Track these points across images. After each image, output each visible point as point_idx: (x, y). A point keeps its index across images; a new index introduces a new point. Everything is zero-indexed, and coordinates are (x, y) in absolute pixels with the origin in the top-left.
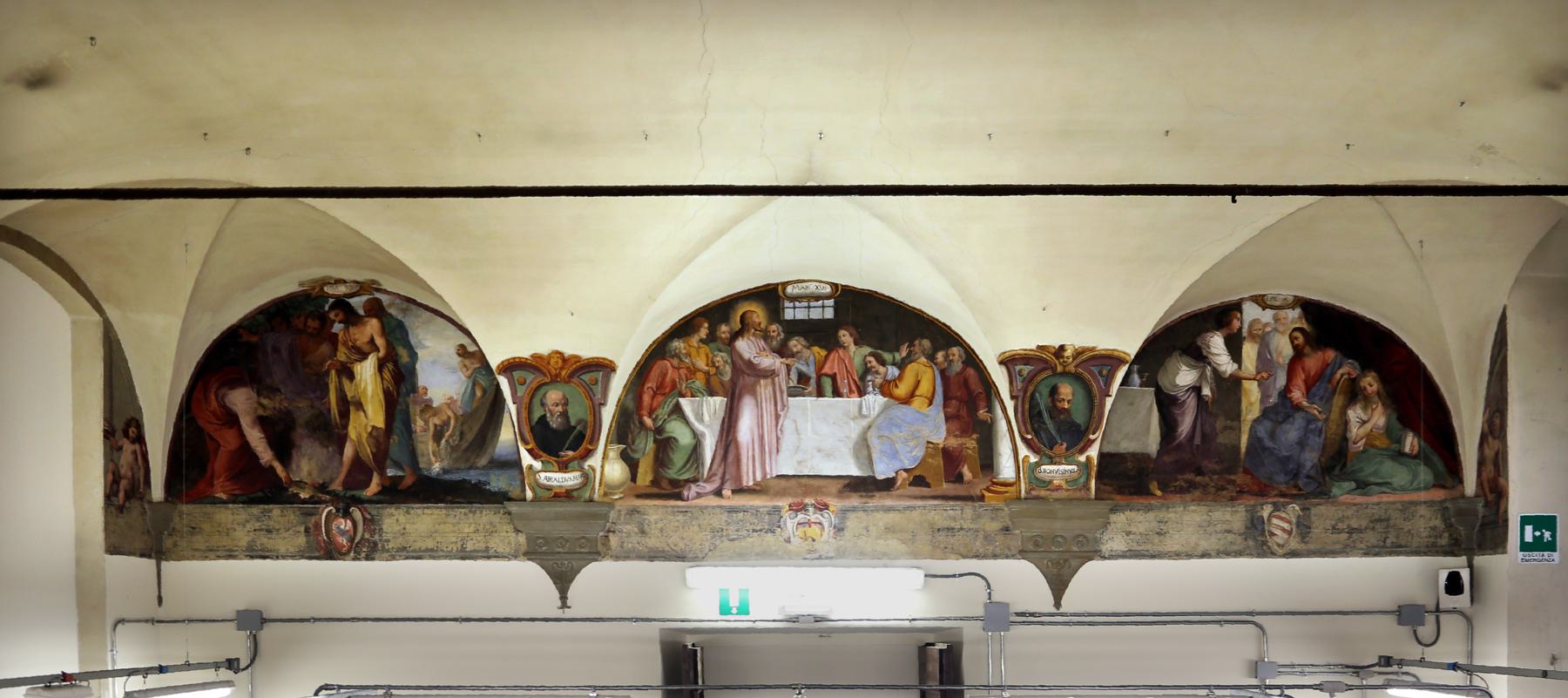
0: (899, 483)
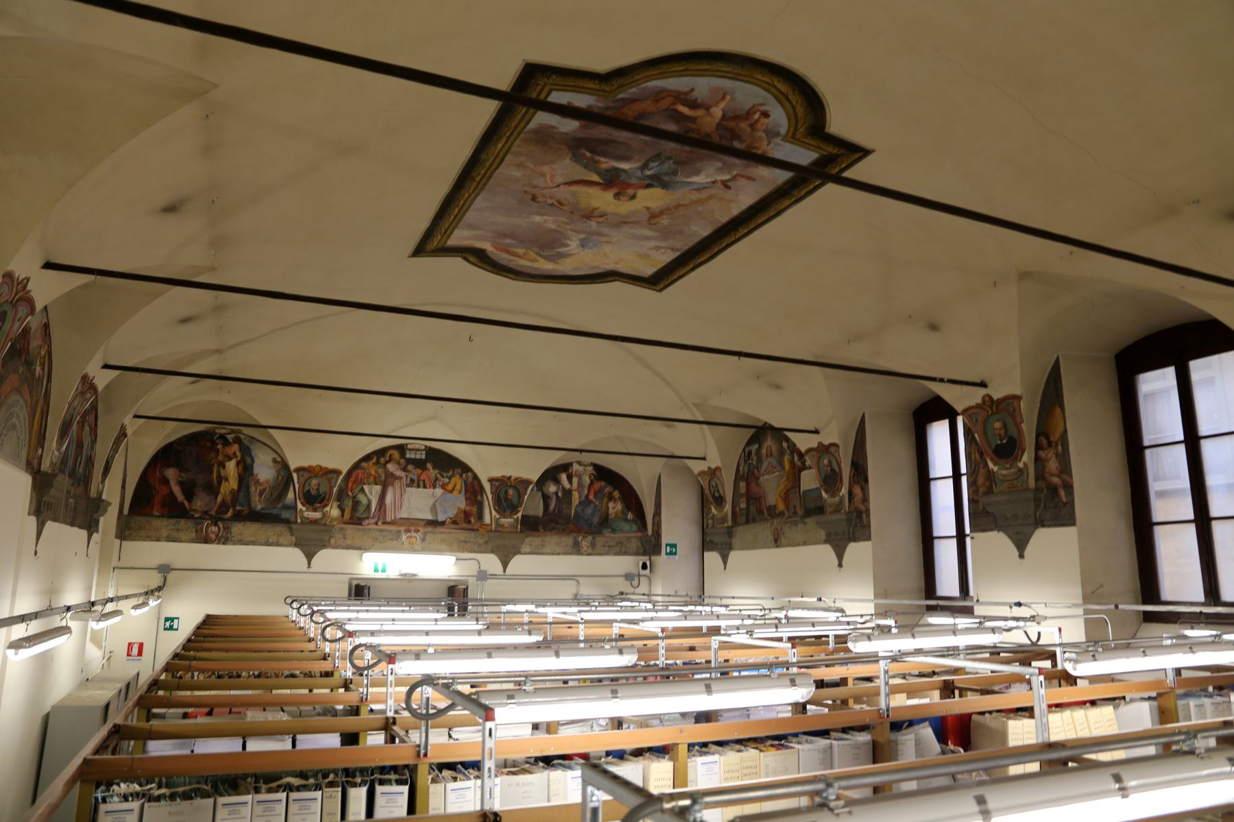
0: (447, 523)
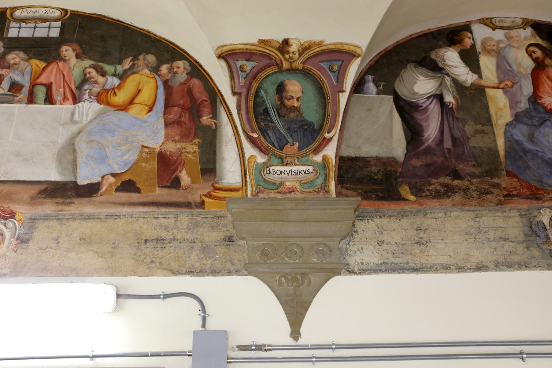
0: (104, 189)
